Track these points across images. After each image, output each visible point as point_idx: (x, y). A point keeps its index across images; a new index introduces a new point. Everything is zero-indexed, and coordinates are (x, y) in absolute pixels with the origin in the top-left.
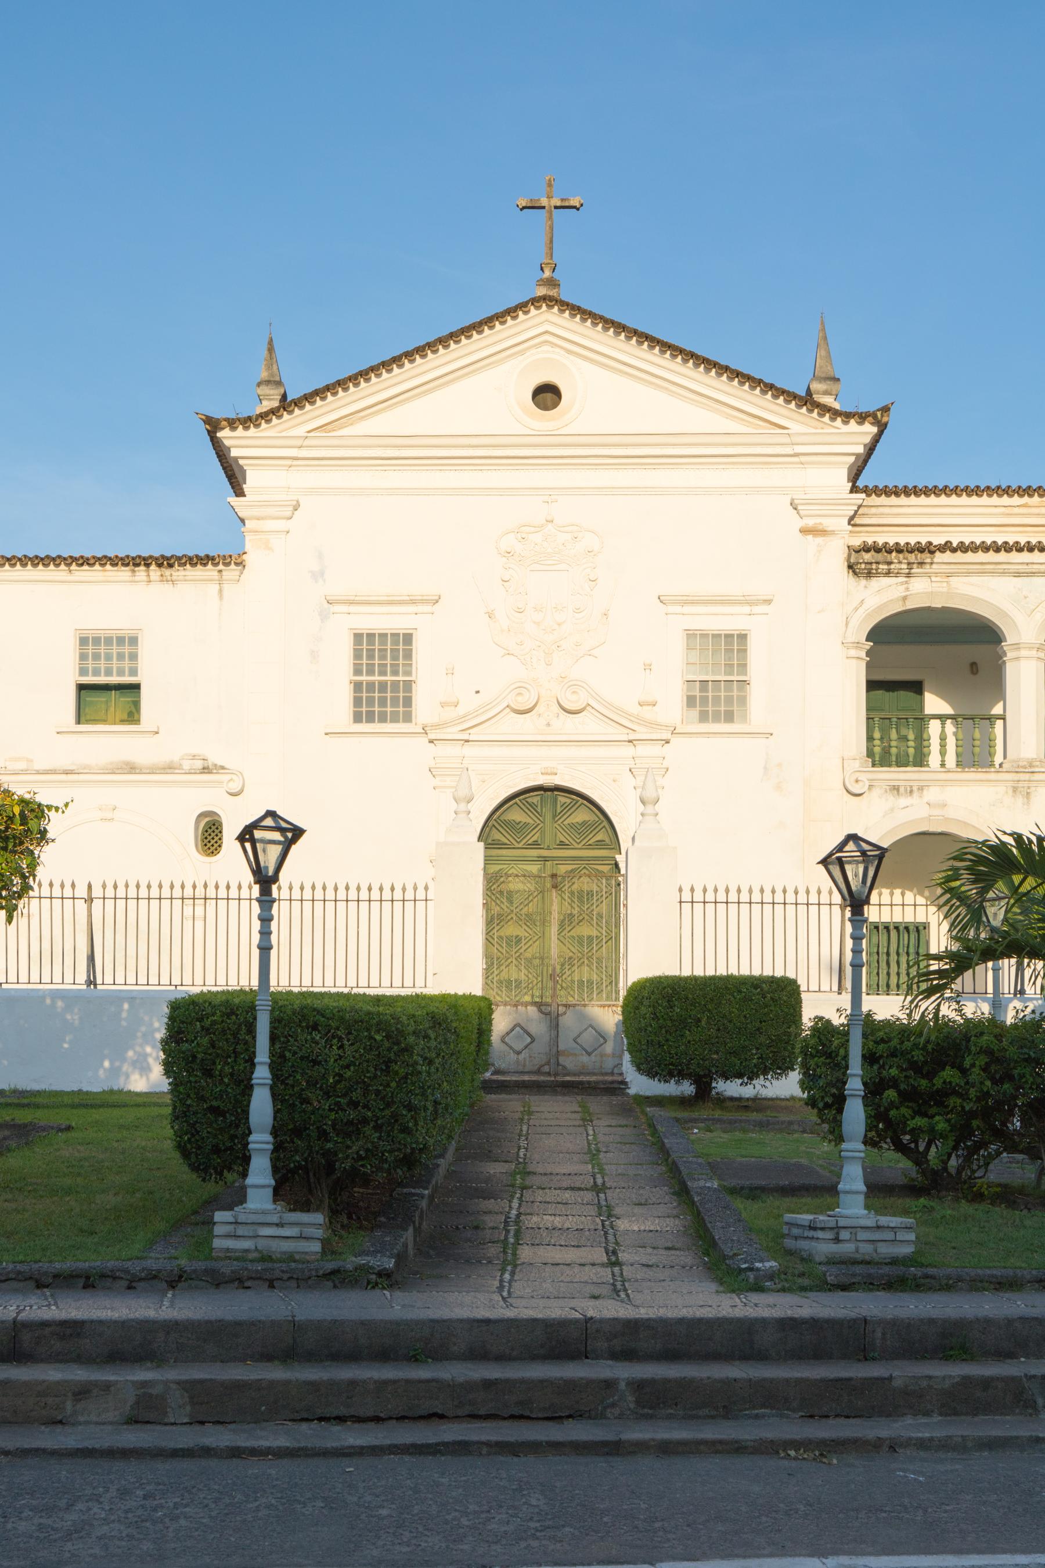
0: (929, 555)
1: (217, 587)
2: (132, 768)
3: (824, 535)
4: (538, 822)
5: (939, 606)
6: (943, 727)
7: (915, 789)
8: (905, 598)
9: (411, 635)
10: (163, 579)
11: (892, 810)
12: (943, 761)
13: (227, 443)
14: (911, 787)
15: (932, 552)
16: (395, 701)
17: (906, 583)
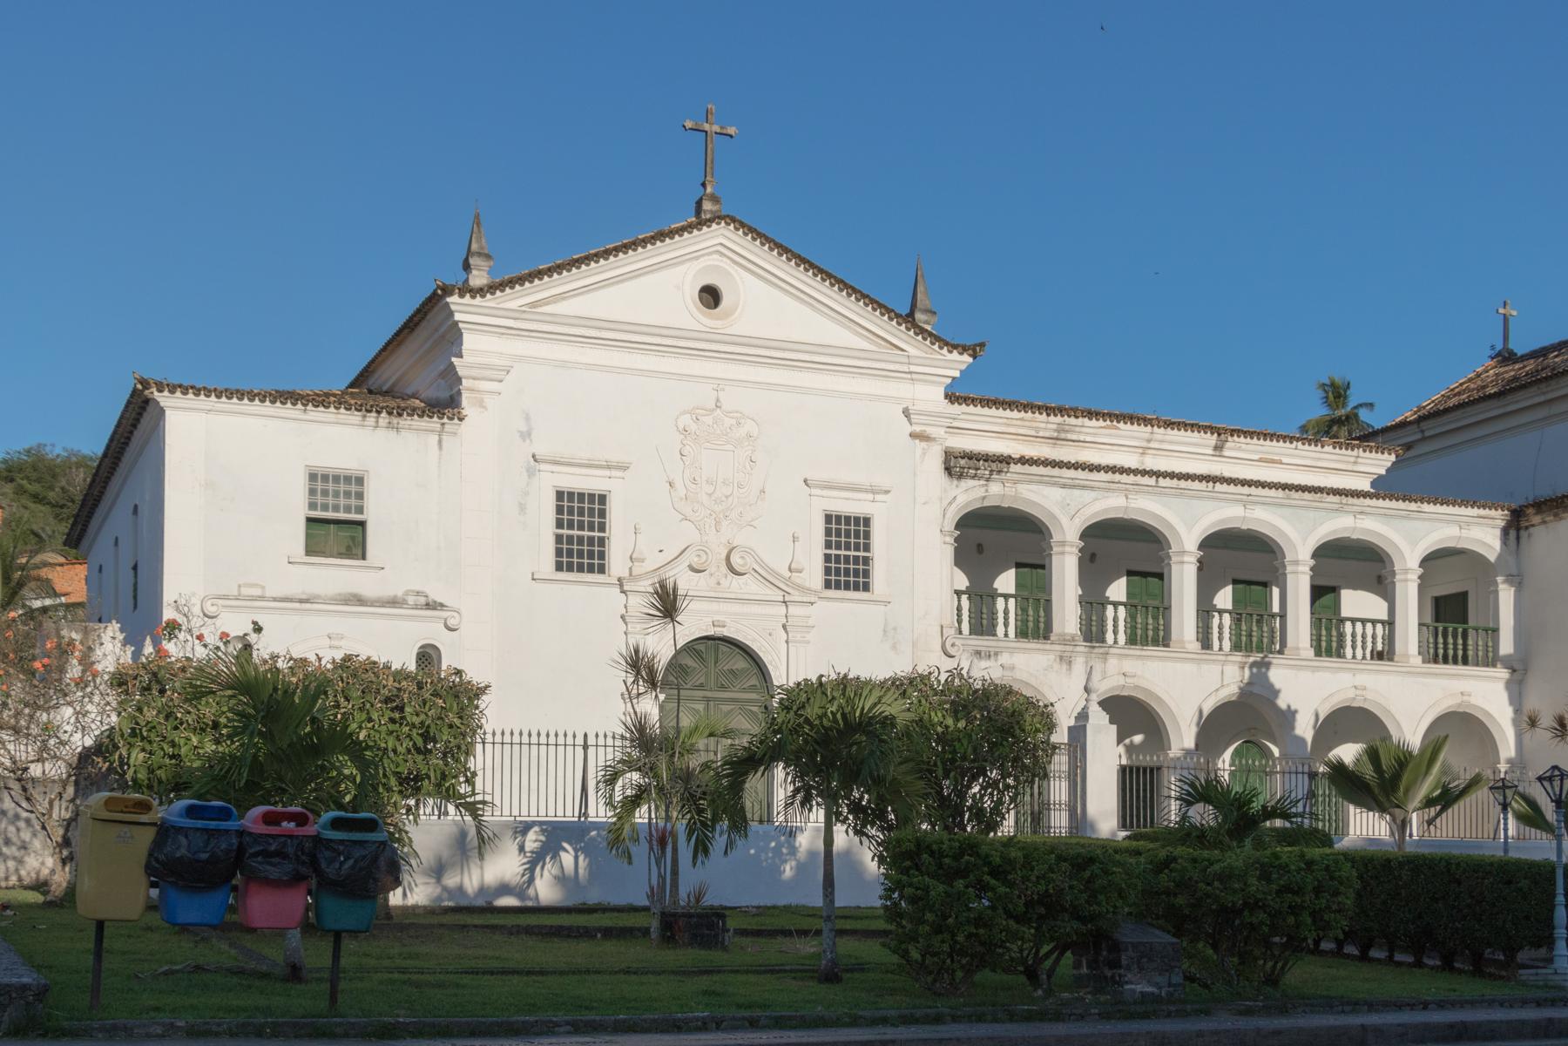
1: (437, 437)
2: (360, 600)
7: (992, 653)
8: (984, 498)
10: (390, 426)
12: (1006, 631)
13: (453, 307)
15: (1008, 464)
16: (591, 555)
17: (986, 485)
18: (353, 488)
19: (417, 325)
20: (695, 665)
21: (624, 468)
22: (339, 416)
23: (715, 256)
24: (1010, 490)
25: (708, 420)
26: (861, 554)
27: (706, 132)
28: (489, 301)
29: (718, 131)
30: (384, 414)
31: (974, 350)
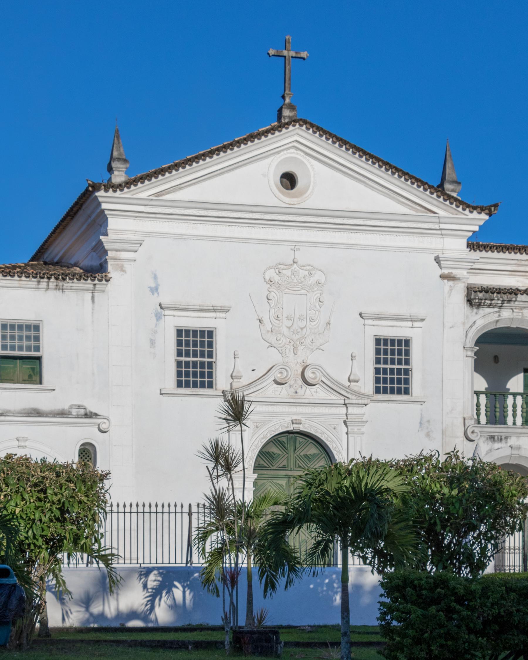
0: (514, 296)
2: (38, 413)
3: (453, 280)
4: (285, 453)
5: (515, 326)
6: (515, 400)
7: (503, 438)
8: (497, 321)
9: (212, 332)
10: (57, 288)
11: (490, 450)
13: (100, 199)
14: (501, 436)
15: (516, 294)
16: (202, 375)
17: (499, 312)
18: (32, 333)
19: (76, 213)
20: (278, 452)
21: (225, 310)
22: (21, 282)
23: (292, 150)
24: (517, 315)
25: (288, 273)
26: (403, 367)
27: (285, 57)
28: (126, 193)
29: (294, 55)
30: (53, 279)
31: (490, 210)
